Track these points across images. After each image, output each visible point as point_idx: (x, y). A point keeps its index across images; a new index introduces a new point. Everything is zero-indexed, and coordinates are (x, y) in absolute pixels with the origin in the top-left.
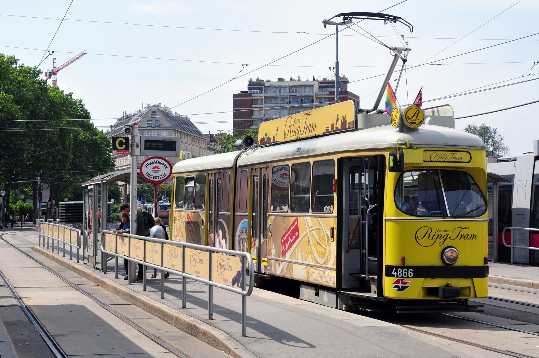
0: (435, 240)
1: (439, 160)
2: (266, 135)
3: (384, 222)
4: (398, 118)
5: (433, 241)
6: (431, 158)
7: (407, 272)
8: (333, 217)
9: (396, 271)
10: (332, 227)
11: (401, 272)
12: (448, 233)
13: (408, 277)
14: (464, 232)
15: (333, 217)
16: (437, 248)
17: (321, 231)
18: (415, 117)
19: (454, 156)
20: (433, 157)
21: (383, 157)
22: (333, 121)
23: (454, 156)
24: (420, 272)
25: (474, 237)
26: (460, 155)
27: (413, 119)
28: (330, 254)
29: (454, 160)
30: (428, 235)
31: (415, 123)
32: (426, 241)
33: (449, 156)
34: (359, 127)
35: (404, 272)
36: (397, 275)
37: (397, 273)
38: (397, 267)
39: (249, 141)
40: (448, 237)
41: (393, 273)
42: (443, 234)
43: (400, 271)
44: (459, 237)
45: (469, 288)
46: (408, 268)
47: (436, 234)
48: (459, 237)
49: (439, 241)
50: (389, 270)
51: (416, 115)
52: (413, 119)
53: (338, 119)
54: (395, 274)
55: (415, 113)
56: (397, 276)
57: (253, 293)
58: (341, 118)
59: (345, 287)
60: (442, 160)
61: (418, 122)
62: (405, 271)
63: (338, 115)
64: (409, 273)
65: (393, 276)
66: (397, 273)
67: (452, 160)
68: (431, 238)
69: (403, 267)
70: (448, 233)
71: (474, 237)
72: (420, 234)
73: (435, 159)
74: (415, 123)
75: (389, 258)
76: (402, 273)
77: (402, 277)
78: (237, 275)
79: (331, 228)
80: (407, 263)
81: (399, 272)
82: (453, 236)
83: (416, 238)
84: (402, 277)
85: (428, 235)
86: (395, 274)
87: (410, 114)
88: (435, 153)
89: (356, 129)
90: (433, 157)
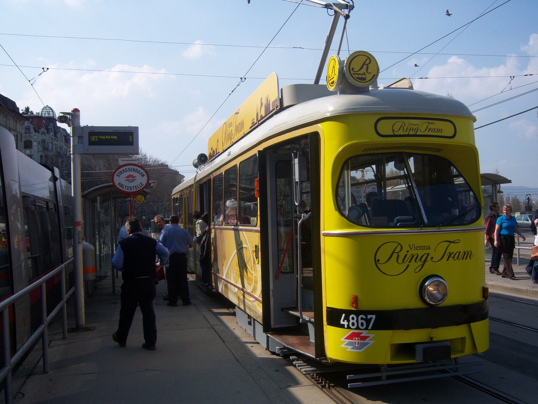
0: (407, 263)
1: (406, 133)
3: (322, 237)
4: (337, 72)
5: (405, 266)
6: (393, 131)
8: (256, 231)
9: (347, 318)
10: (257, 244)
11: (355, 321)
12: (427, 251)
14: (454, 248)
15: (256, 231)
17: (248, 250)
18: (364, 70)
19: (431, 126)
20: (396, 128)
22: (257, 110)
23: (431, 126)
24: (385, 320)
25: (467, 255)
26: (438, 125)
28: (256, 282)
29: (430, 133)
31: (365, 79)
32: (393, 267)
33: (422, 126)
34: (285, 104)
35: (360, 321)
36: (348, 325)
37: (348, 321)
38: (348, 313)
39: (203, 159)
40: (429, 258)
41: (342, 322)
42: (421, 253)
43: (353, 318)
44: (446, 257)
46: (366, 313)
48: (446, 257)
49: (414, 265)
50: (335, 317)
51: (365, 66)
53: (262, 104)
54: (346, 323)
55: (364, 64)
56: (349, 327)
57: (163, 336)
58: (264, 102)
59: (277, 326)
62: (362, 319)
63: (261, 99)
65: (342, 326)
66: (348, 321)
67: (426, 133)
68: (400, 260)
69: (357, 313)
70: (427, 251)
71: (467, 255)
72: (383, 256)
73: (401, 132)
74: (365, 79)
75: (335, 291)
76: (357, 321)
77: (358, 328)
79: (256, 246)
80: (364, 305)
81: (351, 321)
82: (437, 255)
83: (376, 261)
84: (358, 328)
86: (346, 323)
87: (356, 65)
88: (400, 122)
89: (282, 109)
90: (396, 128)
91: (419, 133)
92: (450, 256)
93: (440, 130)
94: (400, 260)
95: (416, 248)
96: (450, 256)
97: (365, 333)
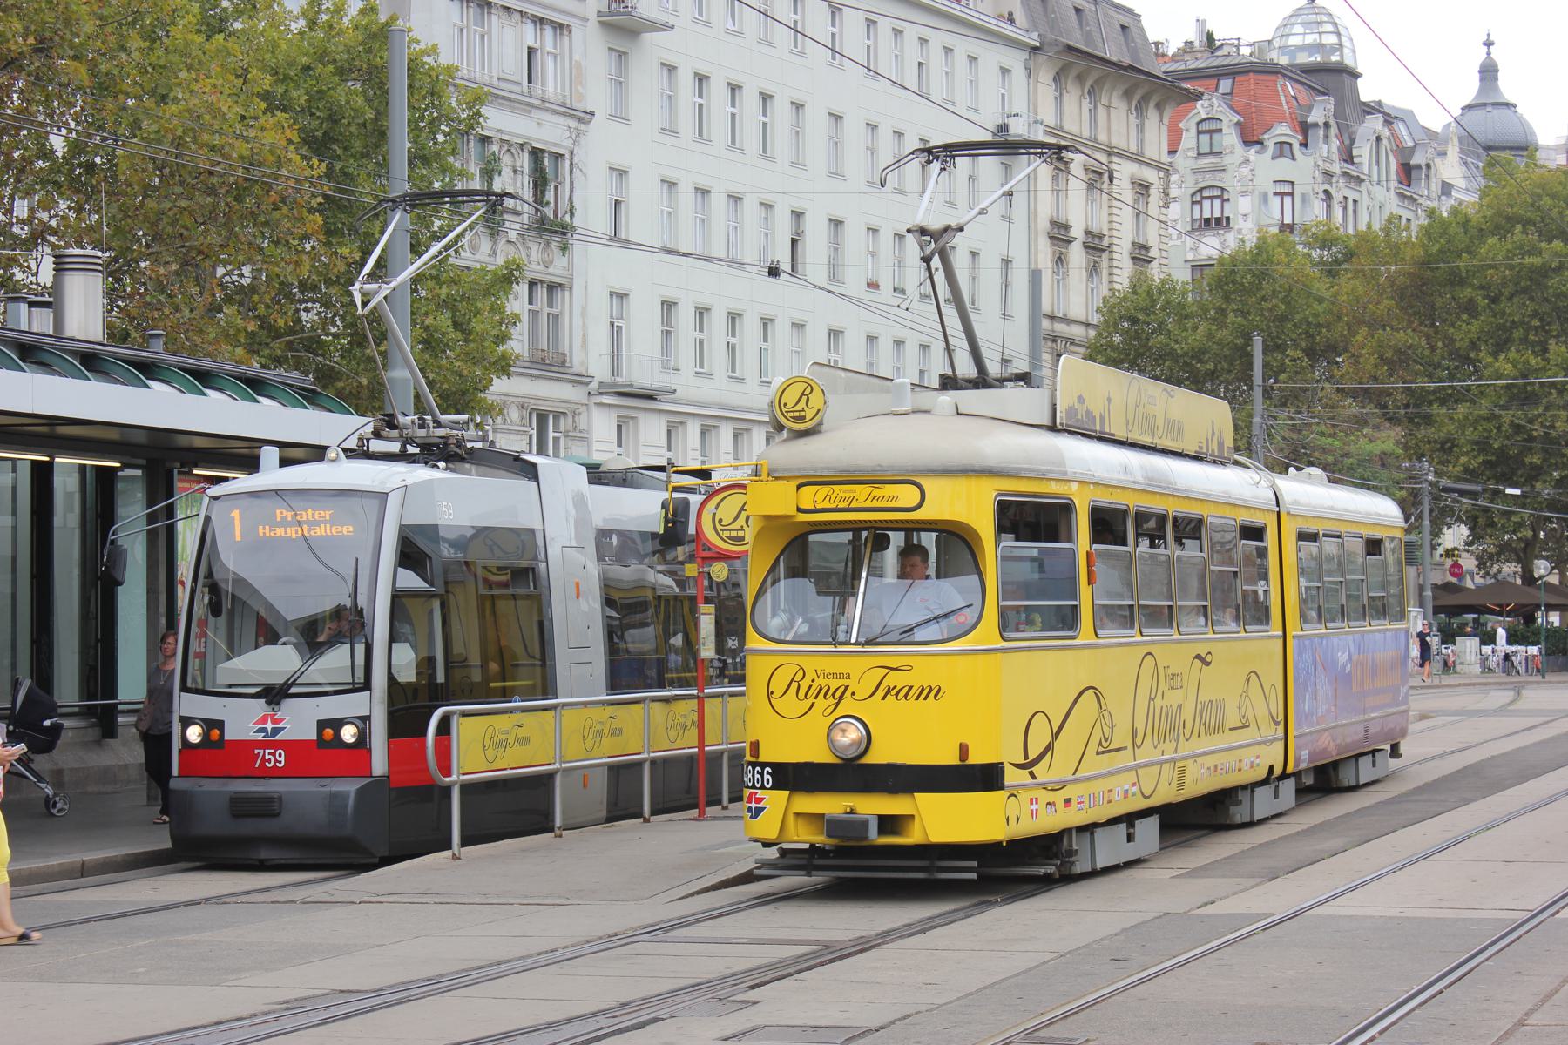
0: (812, 700)
2: (1081, 399)
7: (762, 774)
13: (763, 787)
14: (894, 679)
16: (819, 721)
18: (803, 403)
20: (819, 498)
21: (686, 503)
23: (877, 492)
26: (889, 490)
27: (798, 407)
29: (876, 504)
30: (794, 685)
33: (861, 494)
42: (834, 684)
44: (880, 693)
45: (912, 817)
46: (763, 765)
47: (815, 685)
48: (880, 693)
49: (821, 703)
52: (798, 407)
60: (842, 505)
61: (809, 414)
64: (766, 776)
67: (868, 504)
68: (802, 695)
70: (846, 682)
73: (826, 505)
78: (1204, 796)
80: (762, 759)
85: (794, 685)
87: (790, 398)
88: (825, 489)
90: (819, 498)
91: (854, 505)
92: (889, 691)
93: (891, 498)
94: (802, 695)
95: (826, 676)
96: (889, 691)
97: (760, 793)
